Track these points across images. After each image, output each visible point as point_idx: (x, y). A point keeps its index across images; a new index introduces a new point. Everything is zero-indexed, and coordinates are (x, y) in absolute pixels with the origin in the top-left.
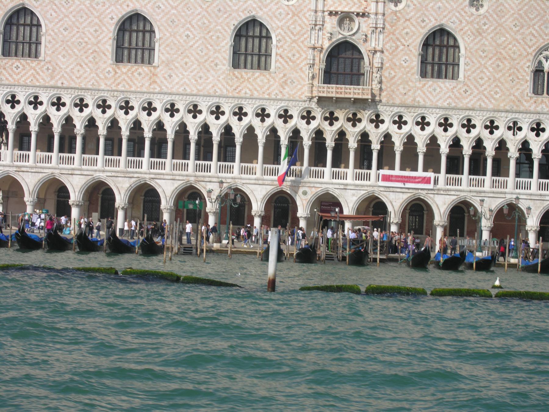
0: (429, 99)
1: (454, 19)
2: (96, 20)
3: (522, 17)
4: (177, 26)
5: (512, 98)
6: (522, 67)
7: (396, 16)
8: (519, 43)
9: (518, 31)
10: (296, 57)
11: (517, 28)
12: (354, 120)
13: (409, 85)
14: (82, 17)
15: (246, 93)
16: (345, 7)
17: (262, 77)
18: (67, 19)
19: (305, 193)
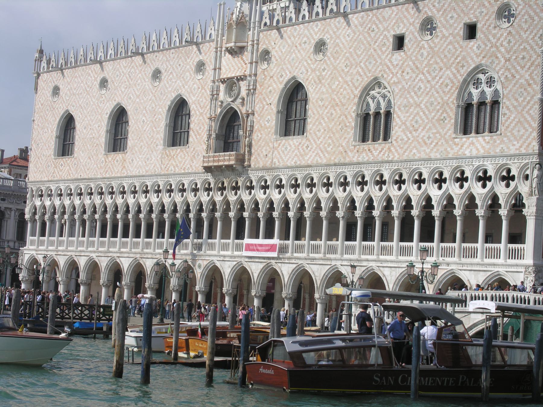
0: (283, 160)
1: (303, 69)
2: (100, 117)
3: (352, 56)
4: (139, 112)
5: (341, 148)
6: (349, 112)
7: (264, 75)
8: (348, 85)
9: (348, 72)
10: (201, 130)
11: (348, 68)
12: (236, 188)
13: (269, 146)
14: (93, 115)
15: (171, 170)
16: (232, 73)
17: (181, 153)
18: (86, 119)
19: (200, 266)
